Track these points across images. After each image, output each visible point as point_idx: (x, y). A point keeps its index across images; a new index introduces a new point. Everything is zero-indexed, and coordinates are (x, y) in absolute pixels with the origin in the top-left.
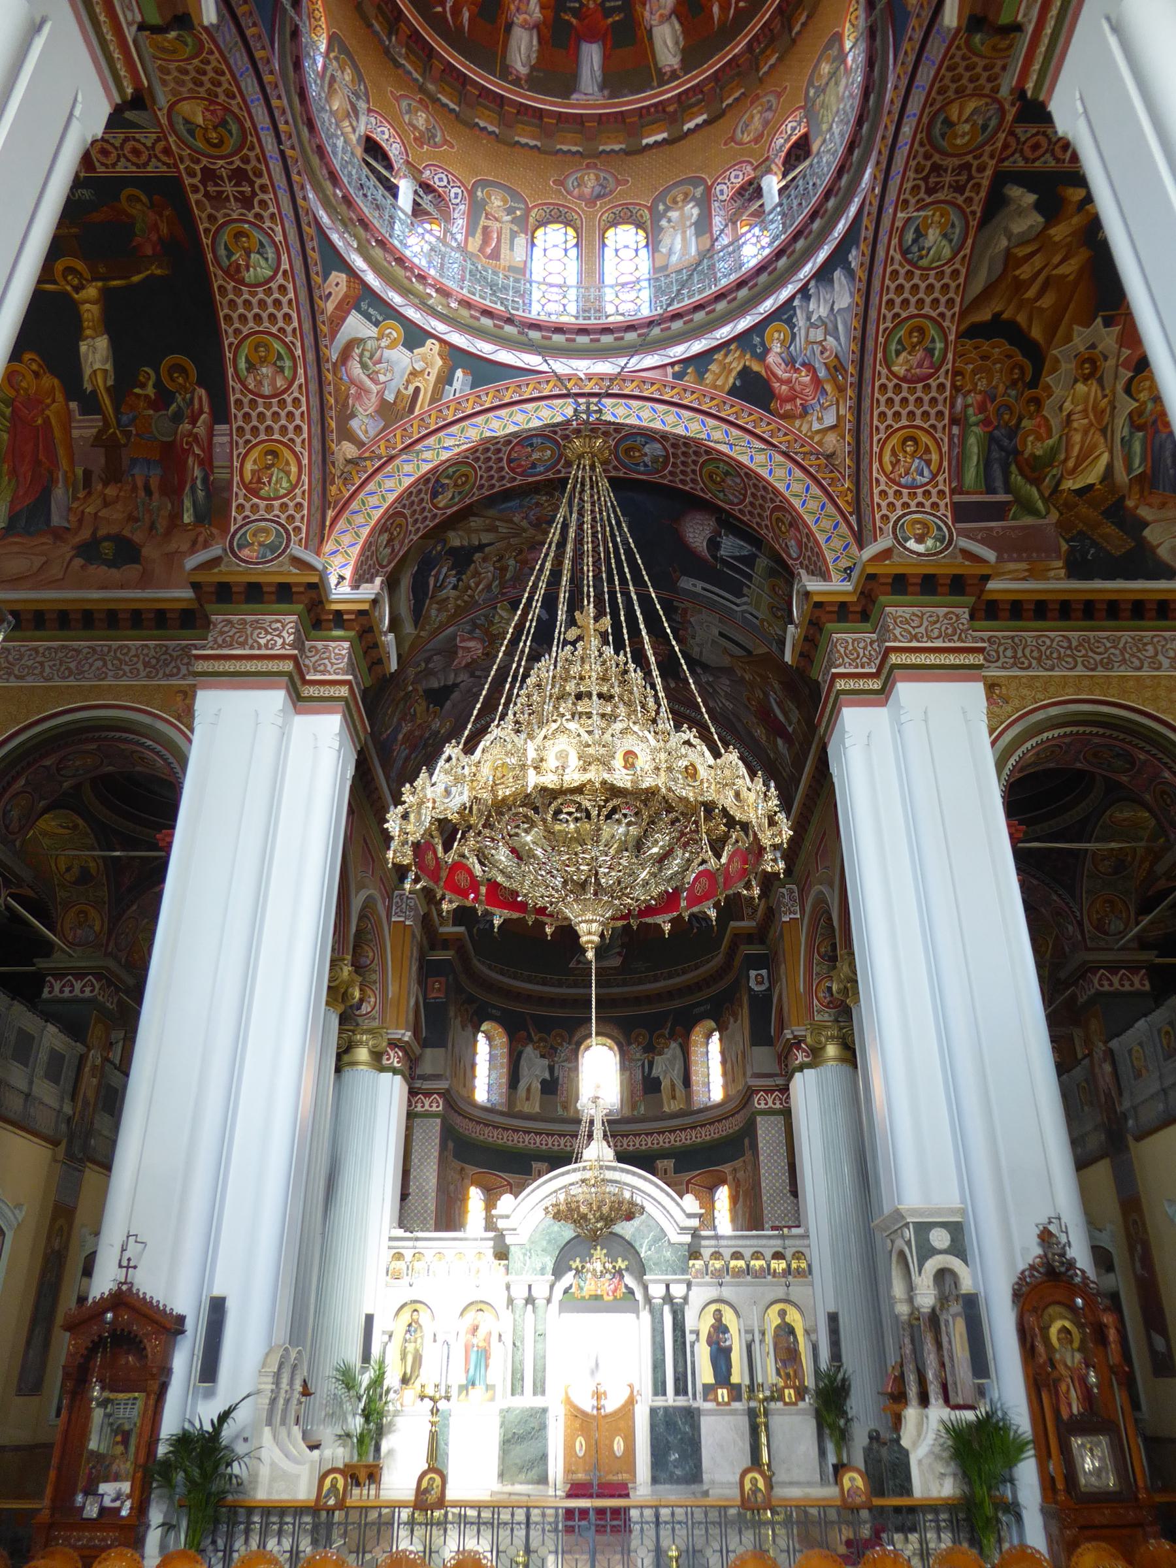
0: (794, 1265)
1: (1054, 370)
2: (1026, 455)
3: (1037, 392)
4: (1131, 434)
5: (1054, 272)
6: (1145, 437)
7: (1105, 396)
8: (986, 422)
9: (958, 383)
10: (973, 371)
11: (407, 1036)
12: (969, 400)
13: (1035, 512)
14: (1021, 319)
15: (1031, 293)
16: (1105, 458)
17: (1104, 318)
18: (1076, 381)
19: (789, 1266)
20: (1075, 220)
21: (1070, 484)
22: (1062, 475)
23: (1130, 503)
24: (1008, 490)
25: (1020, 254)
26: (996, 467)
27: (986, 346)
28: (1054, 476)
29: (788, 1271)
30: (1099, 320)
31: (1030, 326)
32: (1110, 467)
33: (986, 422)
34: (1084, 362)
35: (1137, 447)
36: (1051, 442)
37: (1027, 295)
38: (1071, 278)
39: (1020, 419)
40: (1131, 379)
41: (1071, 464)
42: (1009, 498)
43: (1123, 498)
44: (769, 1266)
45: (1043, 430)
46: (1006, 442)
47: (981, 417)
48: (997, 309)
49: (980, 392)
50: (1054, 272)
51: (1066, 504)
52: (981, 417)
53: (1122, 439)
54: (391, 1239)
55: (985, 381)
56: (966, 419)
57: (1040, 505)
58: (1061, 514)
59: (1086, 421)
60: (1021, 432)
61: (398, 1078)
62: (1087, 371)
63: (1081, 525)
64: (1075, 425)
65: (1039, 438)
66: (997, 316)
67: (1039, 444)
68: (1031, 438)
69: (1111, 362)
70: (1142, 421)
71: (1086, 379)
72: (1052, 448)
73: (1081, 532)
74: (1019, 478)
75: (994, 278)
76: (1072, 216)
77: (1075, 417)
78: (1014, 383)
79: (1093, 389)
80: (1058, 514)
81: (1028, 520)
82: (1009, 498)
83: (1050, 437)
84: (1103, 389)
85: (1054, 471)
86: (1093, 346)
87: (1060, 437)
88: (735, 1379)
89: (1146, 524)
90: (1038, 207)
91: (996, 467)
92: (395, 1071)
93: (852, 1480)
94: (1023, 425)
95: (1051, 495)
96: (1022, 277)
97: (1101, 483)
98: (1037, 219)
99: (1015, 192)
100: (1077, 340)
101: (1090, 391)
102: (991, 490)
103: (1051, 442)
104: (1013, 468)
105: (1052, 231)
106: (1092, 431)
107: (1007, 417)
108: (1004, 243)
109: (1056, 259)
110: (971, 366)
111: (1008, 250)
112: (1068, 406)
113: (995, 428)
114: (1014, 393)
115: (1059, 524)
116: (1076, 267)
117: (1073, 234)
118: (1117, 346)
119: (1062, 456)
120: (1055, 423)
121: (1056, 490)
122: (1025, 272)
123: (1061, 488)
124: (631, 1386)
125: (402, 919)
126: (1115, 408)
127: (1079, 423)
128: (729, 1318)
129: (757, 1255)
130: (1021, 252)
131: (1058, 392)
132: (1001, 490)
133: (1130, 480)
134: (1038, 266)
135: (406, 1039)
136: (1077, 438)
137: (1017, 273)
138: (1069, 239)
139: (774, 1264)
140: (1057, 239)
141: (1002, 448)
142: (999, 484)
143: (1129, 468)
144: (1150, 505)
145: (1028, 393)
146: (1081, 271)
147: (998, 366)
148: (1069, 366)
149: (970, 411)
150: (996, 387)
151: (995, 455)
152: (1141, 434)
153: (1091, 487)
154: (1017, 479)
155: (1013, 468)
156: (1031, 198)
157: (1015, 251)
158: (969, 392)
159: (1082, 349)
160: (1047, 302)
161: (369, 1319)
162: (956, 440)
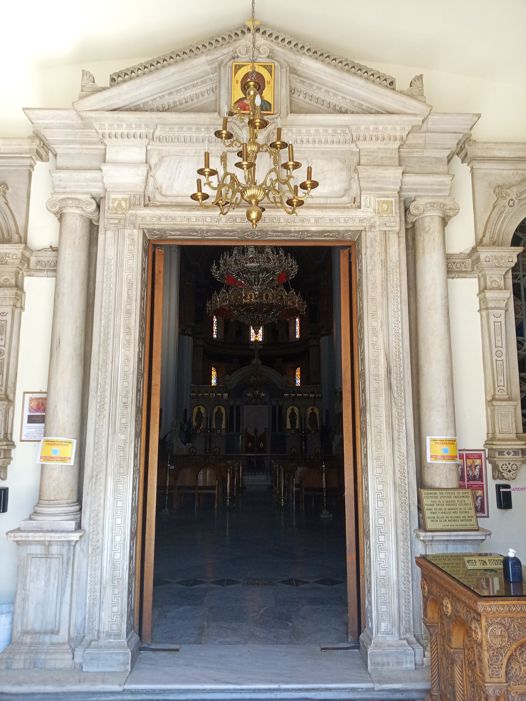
0: (317, 396)
11: (193, 324)
19: (315, 395)
29: (315, 397)
44: (309, 395)
54: (191, 387)
61: (191, 338)
88: (297, 427)
92: (189, 335)
93: (318, 450)
124: (265, 429)
125: (189, 283)
128: (296, 410)
129: (306, 393)
135: (193, 325)
139: (311, 395)
161: (186, 410)
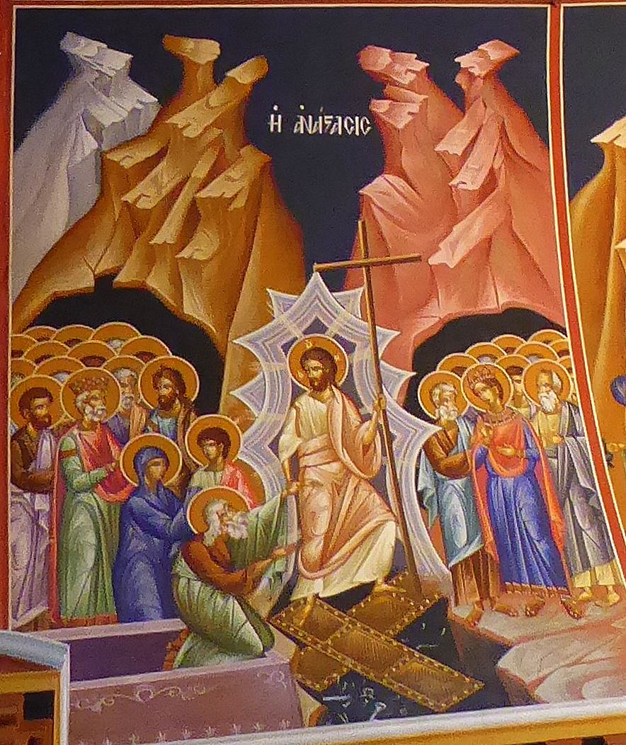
1: (247, 376)
2: (209, 540)
3: (221, 418)
4: (437, 483)
5: (203, 194)
6: (470, 486)
7: (365, 418)
8: (111, 483)
9: (41, 412)
10: (70, 386)
12: (69, 443)
13: (243, 649)
14: (158, 283)
15: (167, 233)
16: (390, 533)
17: (322, 272)
18: (297, 393)
20: (216, 98)
21: (314, 588)
22: (296, 572)
23: (460, 612)
24: (170, 608)
25: (127, 164)
26: (141, 566)
27: (92, 337)
28: (280, 575)
30: (316, 277)
31: (179, 296)
32: (403, 551)
33: (111, 483)
34: (306, 356)
35: (455, 507)
36: (263, 511)
37: (158, 240)
38: (240, 203)
39: (188, 474)
40: (413, 384)
41: (314, 549)
42: (175, 625)
43: (443, 603)
45: (241, 491)
46: (161, 519)
47: (100, 473)
48: (105, 266)
49: (93, 425)
50: (203, 194)
51: (311, 626)
52: (100, 473)
53: (420, 495)
55: (99, 405)
56: (65, 479)
57: (249, 633)
58: (301, 645)
59: (335, 466)
60: (191, 500)
62: (316, 374)
63: (349, 663)
64: (311, 475)
65: (234, 504)
66: (104, 281)
67: (237, 518)
68: (218, 507)
69: (362, 355)
70: (456, 458)
71: (318, 388)
72: (268, 524)
73: (351, 676)
74: (197, 585)
75: (85, 207)
76: (207, 91)
77: (304, 462)
78: (165, 406)
79: (338, 408)
80: (292, 646)
81: (226, 664)
82: (175, 625)
83: (262, 502)
84: (358, 405)
85: (279, 566)
86: (317, 327)
87: (283, 502)
89: (502, 648)
90: (137, 73)
91: (141, 566)
94: (195, 483)
95: (275, 610)
96: (140, 205)
97: (387, 580)
98: (140, 99)
99: (83, 48)
100: (280, 318)
101: (330, 410)
102: (127, 613)
103: (263, 511)
104: (182, 567)
105: (178, 119)
106: (351, 487)
107: (157, 471)
108: (90, 144)
109: (201, 171)
110: (66, 377)
111: (101, 156)
112: (289, 442)
113: (135, 492)
114: (166, 423)
115: (296, 665)
116: (245, 184)
117: (215, 124)
118: (368, 325)
119: (294, 537)
120: (269, 474)
121: (284, 601)
122: (145, 195)
123: (293, 598)
126: (391, 438)
127: (318, 470)
130: (129, 159)
131: (262, 416)
132: (154, 613)
133: (453, 570)
134: (168, 183)
136: (321, 500)
137: (129, 197)
138: (217, 132)
140: (190, 133)
141: (150, 530)
142: (149, 599)
143: (447, 550)
144: (506, 612)
145: (199, 422)
146: (255, 201)
147: (125, 373)
148: (277, 366)
149: (73, 463)
150: (127, 414)
151: (138, 543)
152: (459, 483)
153: (365, 590)
154: (188, 584)
155: (182, 567)
156: (119, 61)
157: (114, 157)
158: (68, 427)
159: (297, 333)
160: (203, 247)
162: (43, 523)
